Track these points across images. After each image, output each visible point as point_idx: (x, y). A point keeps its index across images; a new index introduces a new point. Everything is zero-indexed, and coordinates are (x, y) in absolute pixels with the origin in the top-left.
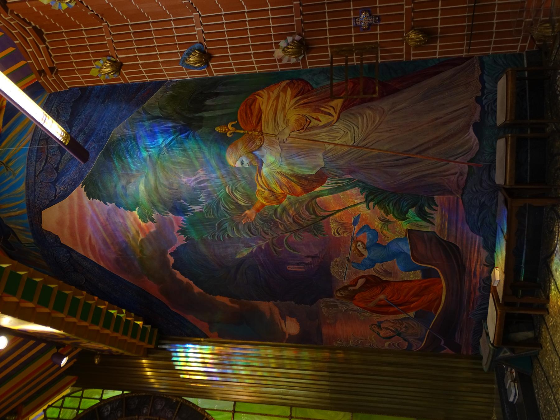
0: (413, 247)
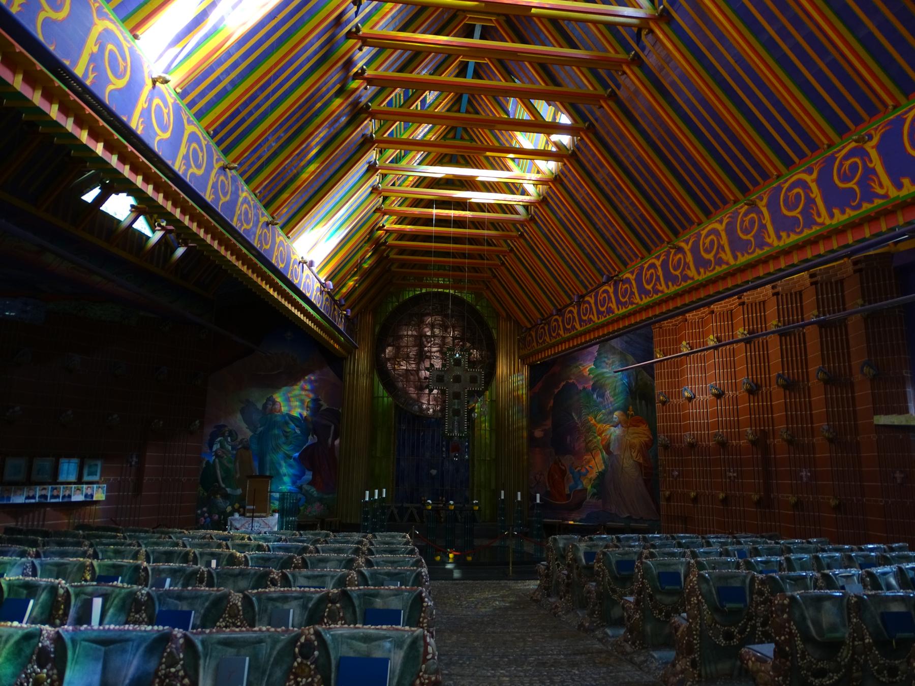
0: (580, 491)
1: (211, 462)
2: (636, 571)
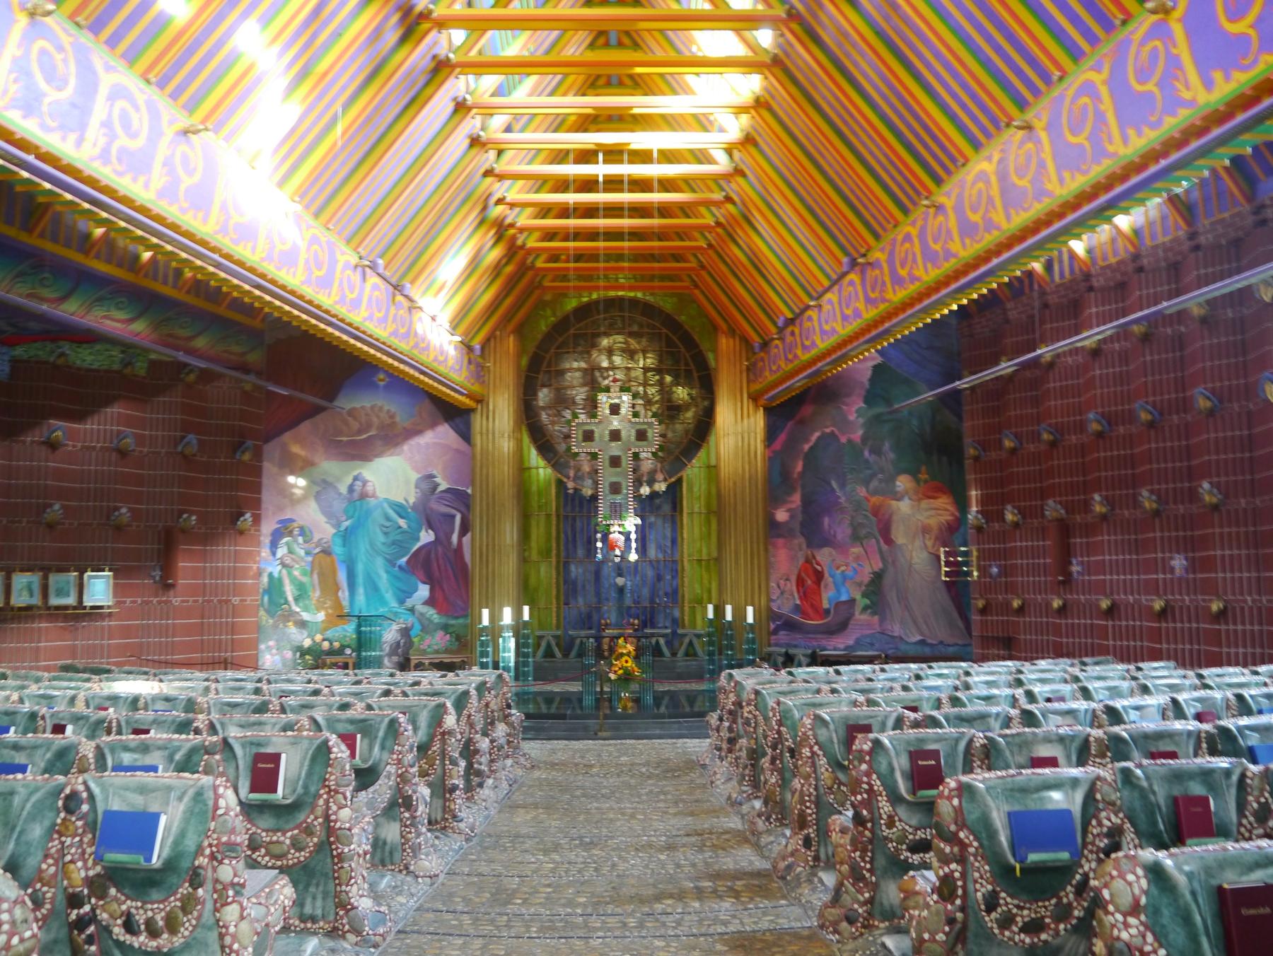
0: (844, 602)
1: (276, 575)
2: (771, 714)
